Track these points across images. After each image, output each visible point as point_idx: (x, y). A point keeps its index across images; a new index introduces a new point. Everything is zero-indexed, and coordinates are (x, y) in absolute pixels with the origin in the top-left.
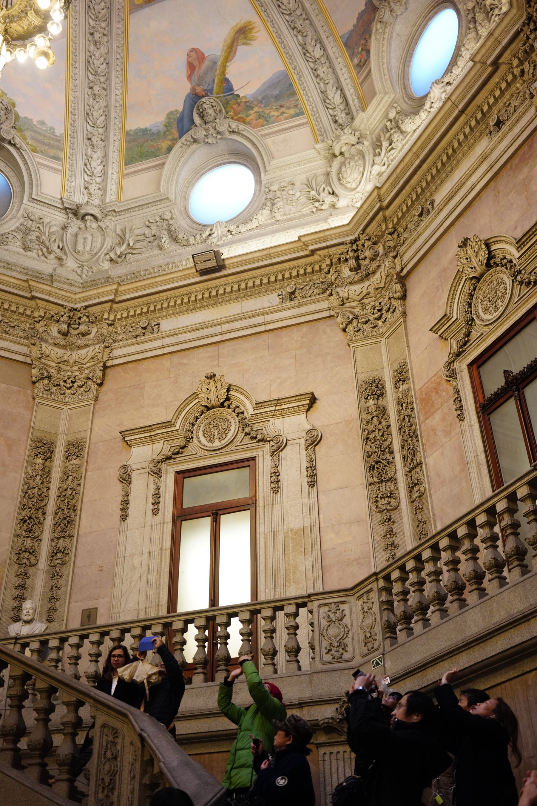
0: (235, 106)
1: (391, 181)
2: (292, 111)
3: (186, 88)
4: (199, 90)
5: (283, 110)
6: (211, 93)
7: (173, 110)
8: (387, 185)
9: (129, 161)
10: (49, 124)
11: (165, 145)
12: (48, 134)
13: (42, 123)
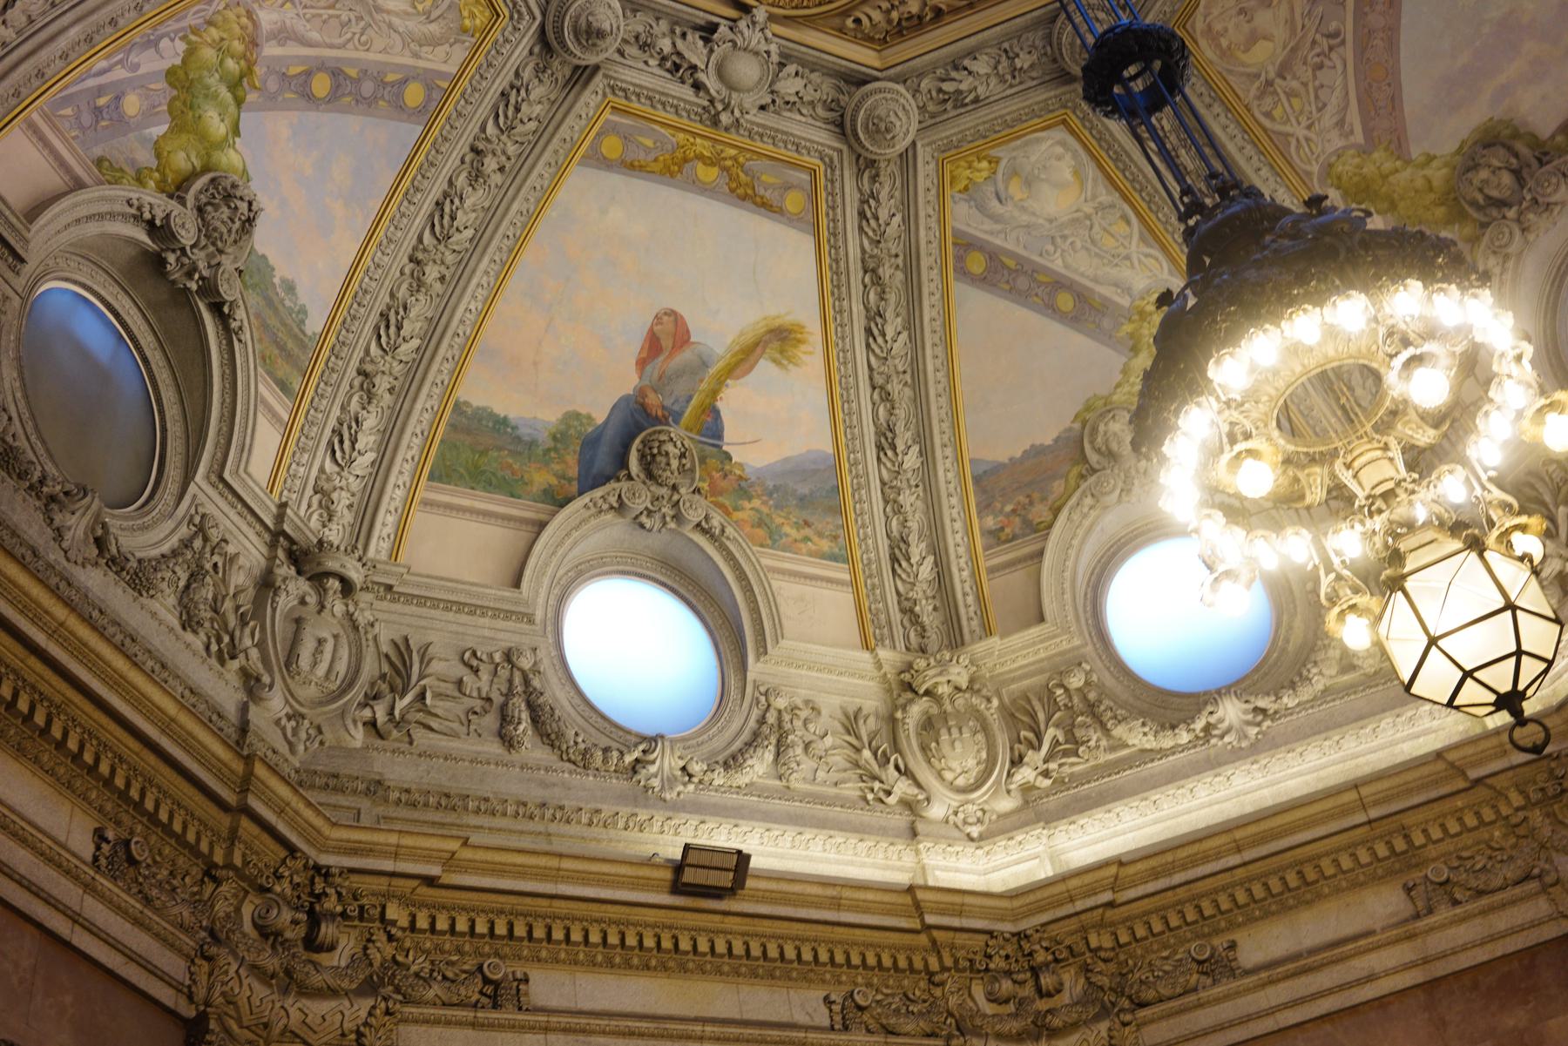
0: (716, 475)
1: (1153, 862)
2: (825, 545)
3: (627, 382)
4: (653, 400)
5: (807, 531)
6: (677, 422)
7: (583, 411)
8: (1140, 866)
9: (441, 474)
10: (304, 296)
11: (541, 478)
12: (289, 321)
13: (290, 288)
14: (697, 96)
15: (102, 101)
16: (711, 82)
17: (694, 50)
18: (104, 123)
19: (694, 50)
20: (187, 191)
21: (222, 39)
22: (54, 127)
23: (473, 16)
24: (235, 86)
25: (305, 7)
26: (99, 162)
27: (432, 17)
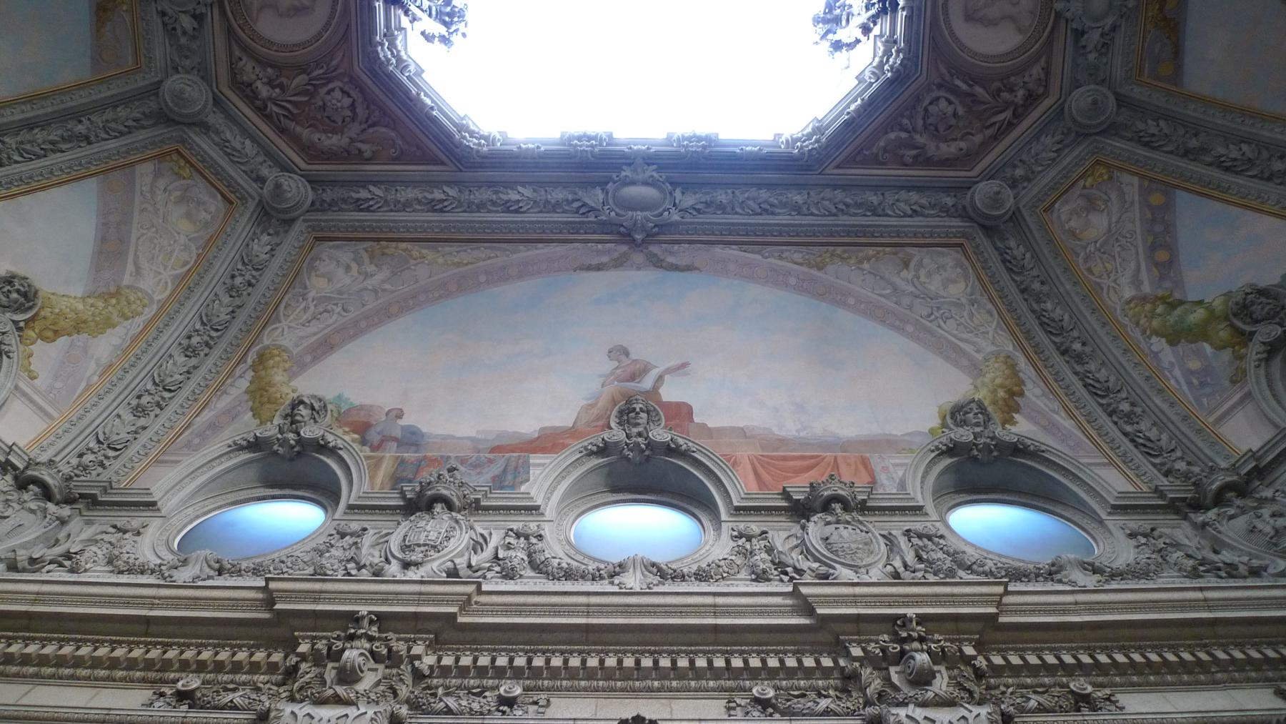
14: (1120, 26)
15: (1195, 381)
16: (1109, 21)
17: (1094, 38)
18: (1209, 380)
19: (1094, 38)
20: (1245, 331)
21: (1146, 316)
22: (1215, 409)
23: (1101, 175)
24: (1172, 306)
25: (1117, 272)
26: (1233, 382)
27: (1106, 198)
